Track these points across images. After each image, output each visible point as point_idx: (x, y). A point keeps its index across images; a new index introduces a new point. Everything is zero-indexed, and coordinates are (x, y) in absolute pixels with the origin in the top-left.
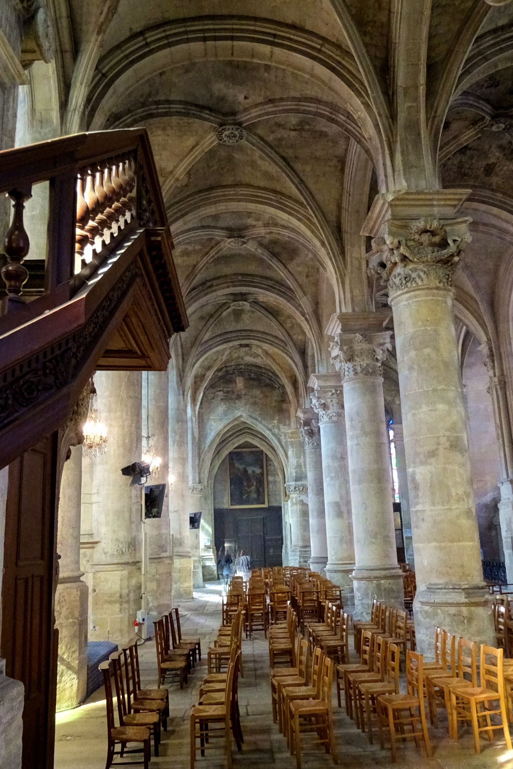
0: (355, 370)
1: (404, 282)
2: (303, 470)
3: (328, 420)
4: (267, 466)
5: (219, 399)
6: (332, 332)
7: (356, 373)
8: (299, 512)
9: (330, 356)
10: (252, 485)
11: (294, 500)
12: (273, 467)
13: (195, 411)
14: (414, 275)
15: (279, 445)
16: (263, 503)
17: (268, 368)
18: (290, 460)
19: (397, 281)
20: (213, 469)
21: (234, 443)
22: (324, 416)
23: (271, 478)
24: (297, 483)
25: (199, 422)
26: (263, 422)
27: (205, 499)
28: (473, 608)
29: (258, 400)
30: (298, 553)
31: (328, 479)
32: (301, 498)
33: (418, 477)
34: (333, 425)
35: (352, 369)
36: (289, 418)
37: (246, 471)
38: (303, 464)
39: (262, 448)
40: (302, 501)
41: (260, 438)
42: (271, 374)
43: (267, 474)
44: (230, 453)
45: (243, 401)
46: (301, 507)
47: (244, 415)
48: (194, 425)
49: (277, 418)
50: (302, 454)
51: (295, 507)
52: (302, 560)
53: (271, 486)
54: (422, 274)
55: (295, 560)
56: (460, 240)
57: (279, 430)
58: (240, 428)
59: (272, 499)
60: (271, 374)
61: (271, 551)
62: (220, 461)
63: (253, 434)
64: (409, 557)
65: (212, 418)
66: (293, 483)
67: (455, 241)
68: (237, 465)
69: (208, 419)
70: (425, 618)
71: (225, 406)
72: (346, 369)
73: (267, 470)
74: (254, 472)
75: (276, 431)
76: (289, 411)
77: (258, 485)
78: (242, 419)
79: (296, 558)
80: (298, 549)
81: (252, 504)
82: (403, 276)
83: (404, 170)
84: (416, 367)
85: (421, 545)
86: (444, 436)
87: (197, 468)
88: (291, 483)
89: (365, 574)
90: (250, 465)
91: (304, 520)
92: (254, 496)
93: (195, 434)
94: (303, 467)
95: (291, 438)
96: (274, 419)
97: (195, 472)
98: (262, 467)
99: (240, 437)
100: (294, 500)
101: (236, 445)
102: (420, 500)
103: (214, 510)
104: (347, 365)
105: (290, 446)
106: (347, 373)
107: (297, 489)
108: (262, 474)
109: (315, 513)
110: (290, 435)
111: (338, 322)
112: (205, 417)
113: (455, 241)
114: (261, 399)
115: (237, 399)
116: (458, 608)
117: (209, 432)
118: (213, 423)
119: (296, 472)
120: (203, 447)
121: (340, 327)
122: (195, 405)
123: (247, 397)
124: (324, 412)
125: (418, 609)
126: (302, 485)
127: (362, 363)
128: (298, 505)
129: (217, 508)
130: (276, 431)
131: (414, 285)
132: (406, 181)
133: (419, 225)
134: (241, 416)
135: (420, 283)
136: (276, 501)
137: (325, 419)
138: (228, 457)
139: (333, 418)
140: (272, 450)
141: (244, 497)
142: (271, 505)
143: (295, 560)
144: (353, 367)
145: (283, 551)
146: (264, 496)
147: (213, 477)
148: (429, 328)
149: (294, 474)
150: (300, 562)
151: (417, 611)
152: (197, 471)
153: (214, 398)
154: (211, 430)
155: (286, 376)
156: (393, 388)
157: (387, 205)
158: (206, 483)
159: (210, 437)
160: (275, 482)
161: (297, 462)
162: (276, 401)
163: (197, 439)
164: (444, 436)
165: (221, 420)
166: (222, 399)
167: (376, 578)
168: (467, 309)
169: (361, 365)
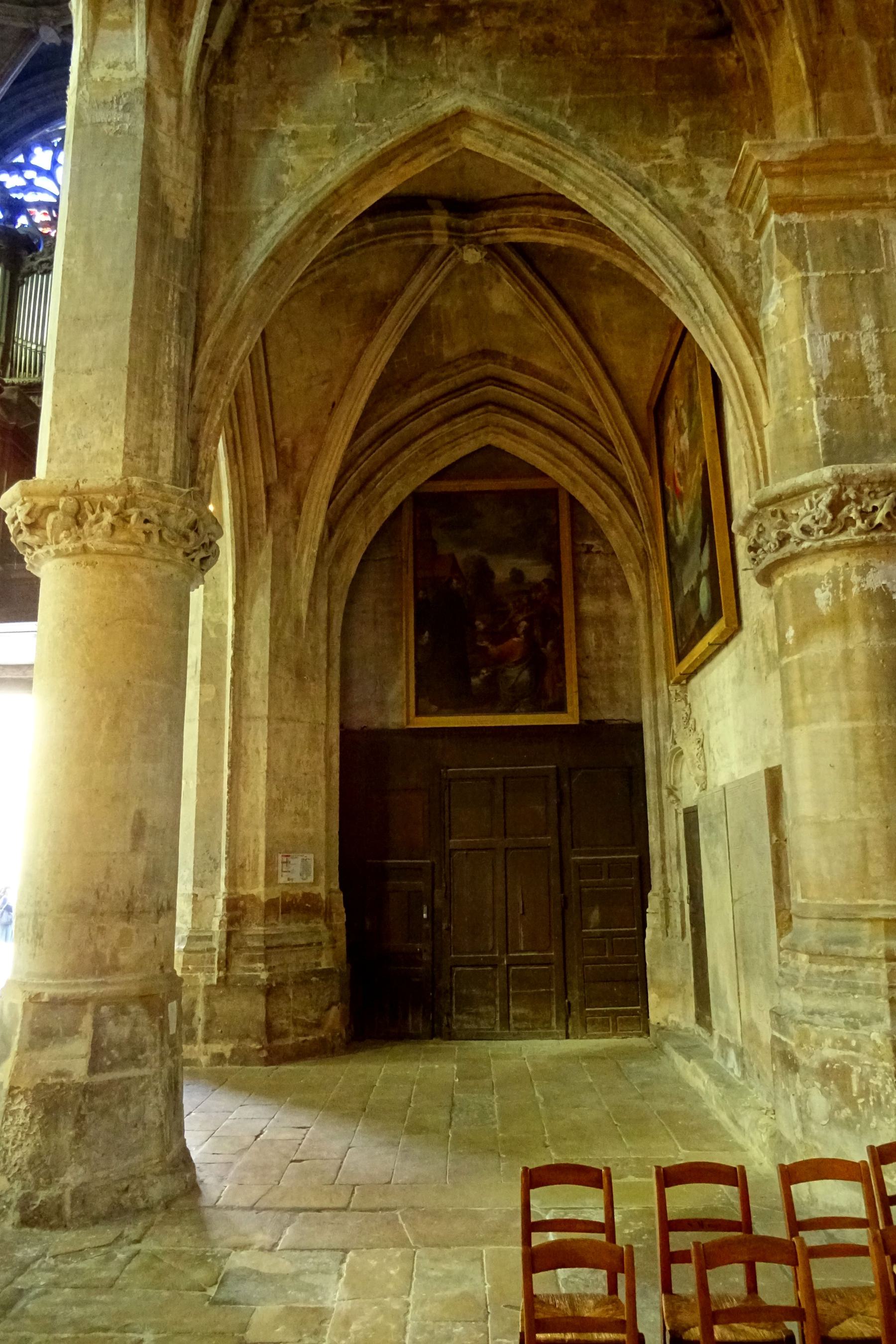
4: (575, 555)
5: (335, 29)
10: (511, 631)
11: (823, 597)
12: (599, 562)
13: (177, 66)
16: (560, 706)
18: (773, 347)
20: (339, 556)
21: (431, 452)
23: (591, 606)
24: (860, 469)
25: (206, 153)
26: (597, 151)
27: (299, 675)
29: (560, 31)
32: (875, 581)
37: (484, 573)
38: (872, 364)
39: (559, 475)
41: (547, 426)
43: (577, 588)
44: (418, 498)
45: (477, 40)
46: (876, 639)
47: (478, 105)
48: (164, 137)
53: (590, 637)
55: (854, 1021)
57: (701, 193)
58: (460, 380)
59: (598, 693)
61: (595, 915)
62: (375, 526)
63: (516, 411)
65: (285, 128)
66: (827, 473)
68: (446, 547)
69: (265, 135)
71: (364, 65)
73: (577, 572)
74: (517, 576)
75: (681, 195)
76: (759, 75)
77: (537, 632)
78: (468, 139)
79: (858, 1004)
81: (510, 709)
87: (168, 389)
88: (805, 478)
90: (502, 547)
92: (519, 675)
93: (166, 187)
94: (876, 382)
95: (780, 204)
97: (155, 414)
98: (552, 557)
99: (461, 423)
100: (823, 597)
101: (442, 462)
103: (348, 737)
105: (778, 258)
108: (554, 585)
110: (781, 186)
112: (242, 122)
114: (583, 27)
115: (437, 27)
117: (265, 203)
118: (293, 158)
119: (829, 416)
120: (222, 289)
122: (180, 32)
123: (497, 19)
128: (859, 632)
129: (356, 726)
130: (681, 195)
134: (462, 117)
136: (614, 698)
138: (407, 514)
140: (598, 477)
141: (475, 681)
142: (593, 716)
143: (854, 1021)
145: (652, 920)
146: (560, 678)
147: (342, 589)
149: (819, 428)
152: (168, 406)
153: (303, 24)
154: (278, 192)
158: (304, 607)
159: (270, 234)
160: (608, 621)
161: (836, 348)
162: (674, 34)
163: (181, 230)
165: (337, 138)
166: (351, 32)
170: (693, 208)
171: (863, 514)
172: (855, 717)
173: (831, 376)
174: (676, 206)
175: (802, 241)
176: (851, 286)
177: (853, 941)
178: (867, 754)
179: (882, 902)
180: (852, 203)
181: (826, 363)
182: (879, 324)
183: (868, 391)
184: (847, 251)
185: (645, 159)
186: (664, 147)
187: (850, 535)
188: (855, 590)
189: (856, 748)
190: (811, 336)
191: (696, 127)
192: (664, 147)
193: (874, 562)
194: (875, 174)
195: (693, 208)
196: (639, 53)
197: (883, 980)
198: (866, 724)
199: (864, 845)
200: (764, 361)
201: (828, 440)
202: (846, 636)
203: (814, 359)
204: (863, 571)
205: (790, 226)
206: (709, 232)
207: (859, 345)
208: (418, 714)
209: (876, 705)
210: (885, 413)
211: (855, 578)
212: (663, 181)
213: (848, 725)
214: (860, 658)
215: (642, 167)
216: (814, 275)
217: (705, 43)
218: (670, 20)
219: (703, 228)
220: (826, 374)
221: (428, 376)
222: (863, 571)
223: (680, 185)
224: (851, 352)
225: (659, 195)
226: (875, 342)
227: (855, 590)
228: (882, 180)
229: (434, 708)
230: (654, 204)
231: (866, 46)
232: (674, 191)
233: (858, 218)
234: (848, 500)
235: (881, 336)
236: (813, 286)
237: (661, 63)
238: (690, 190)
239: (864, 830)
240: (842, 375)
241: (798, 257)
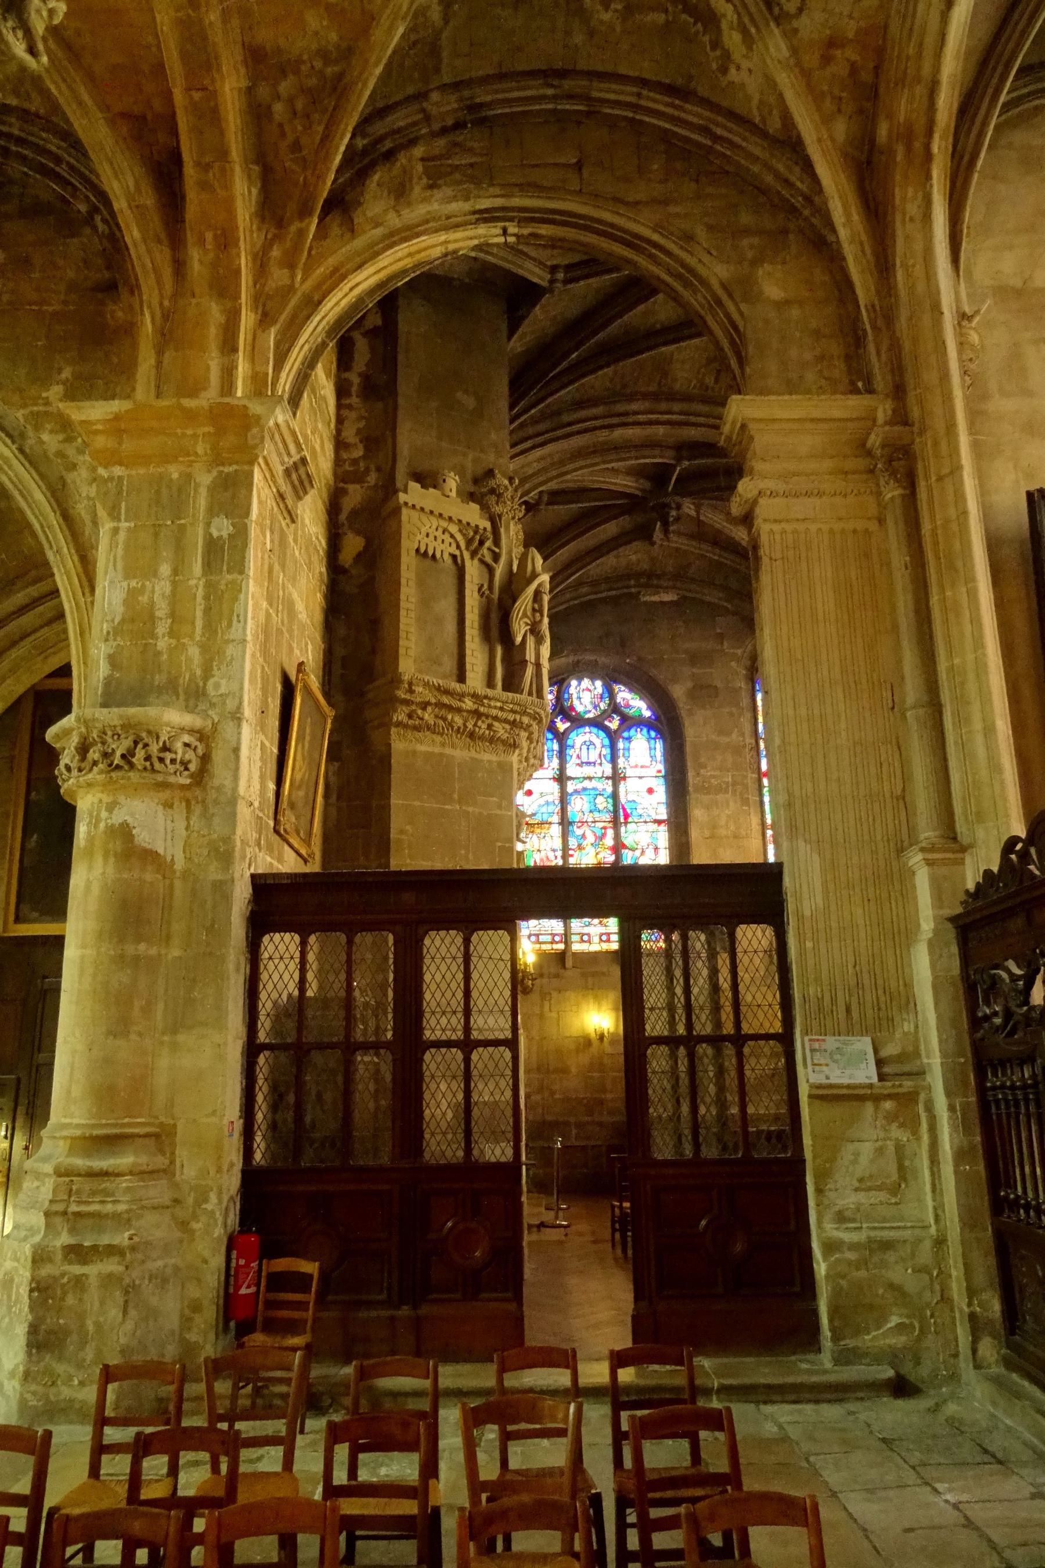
2: (162, 644)
15: (53, 519)
17: (35, 105)
32: (118, 817)
36: (127, 370)
38: (162, 610)
40: (125, 832)
42: (54, 144)
46: (110, 870)
49: (67, 373)
50: (167, 553)
52: (65, 1239)
60: (54, 144)
64: (831, 1230)
91: (120, 960)
94: (162, 629)
96: (45, 382)
107: (94, 754)
126: (128, 726)
150: (40, 1258)
155: (106, 108)
156: (746, 218)
161: (132, 595)
162: (72, 287)
170: (60, 454)
171: (105, 755)
173: (123, 621)
174: (45, 452)
175: (119, 493)
176: (156, 535)
179: (76, 1121)
180: (166, 459)
181: (121, 609)
182: (175, 572)
183: (154, 636)
184: (158, 502)
185: (24, 406)
186: (44, 395)
187: (95, 775)
188: (102, 825)
190: (112, 582)
191: (78, 376)
192: (44, 395)
193: (122, 799)
194: (189, 432)
195: (60, 454)
196: (35, 303)
199: (72, 1069)
200: (92, 603)
201: (108, 682)
202: (90, 868)
203: (110, 604)
204: (111, 808)
205: (111, 479)
206: (70, 477)
207: (153, 592)
208: (18, 920)
209: (100, 935)
210: (165, 657)
211: (104, 814)
212: (37, 428)
214: (96, 889)
215: (20, 414)
216: (124, 525)
217: (100, 295)
218: (71, 274)
219: (64, 473)
220: (117, 621)
221: (33, 573)
223: (51, 432)
224: (144, 599)
225: (31, 441)
226: (168, 590)
227: (102, 825)
228: (195, 436)
229: (35, 915)
230: (21, 450)
231: (213, 305)
232: (45, 437)
233: (174, 472)
234: (94, 743)
235: (174, 584)
236: (122, 536)
237: (54, 314)
238: (61, 437)
240: (133, 620)
241: (114, 508)
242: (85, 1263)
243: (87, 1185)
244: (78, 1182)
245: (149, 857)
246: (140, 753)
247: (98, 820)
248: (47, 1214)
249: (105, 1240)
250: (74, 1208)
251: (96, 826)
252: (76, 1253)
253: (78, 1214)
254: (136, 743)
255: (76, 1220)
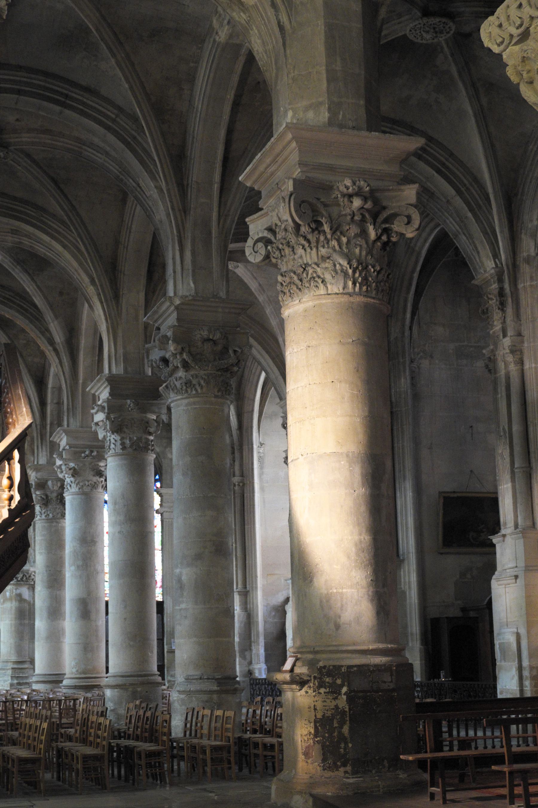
0: (123, 444)
1: (184, 387)
3: (77, 490)
6: (96, 391)
7: (124, 448)
8: (13, 611)
9: (93, 421)
14: (194, 382)
19: (178, 384)
22: (73, 485)
28: (223, 695)
30: (10, 672)
31: (73, 568)
32: (18, 591)
33: (184, 578)
34: (83, 497)
35: (119, 442)
51: (8, 605)
52: (15, 682)
54: (202, 382)
56: (240, 351)
64: (170, 678)
67: (235, 351)
70: (181, 706)
72: (113, 441)
79: (6, 678)
80: (10, 665)
82: (184, 380)
83: (193, 271)
84: (190, 473)
85: (182, 641)
86: (210, 541)
89: (119, 681)
91: (21, 624)
102: (184, 599)
104: (113, 436)
106: (112, 446)
109: (45, 614)
111: (106, 383)
113: (235, 351)
116: (209, 696)
121: (108, 390)
124: (72, 479)
125: (176, 698)
127: (131, 436)
128: (14, 602)
131: (194, 392)
132: (194, 283)
133: (202, 333)
135: (199, 390)
137: (74, 489)
139: (84, 488)
144: (121, 440)
148: (205, 436)
151: (174, 701)
157: (172, 308)
164: (210, 541)
167: (131, 684)
168: (267, 352)
169: (130, 438)
172: (11, 620)
177: (7, 666)
178: (13, 629)
188: (14, 594)
189: (11, 628)
197: (11, 673)
198: (13, 622)
202: (11, 603)
204: (16, 589)
209: (16, 618)
211: (14, 591)
213: (10, 622)
214: (14, 608)
222: (16, 589)
239: (11, 644)
242: (21, 685)
243: (19, 671)
244: (17, 671)
245: (25, 600)
246: (25, 578)
247: (13, 592)
248: (12, 677)
249: (25, 681)
250: (17, 675)
251: (12, 593)
252: (19, 684)
253: (18, 677)
254: (23, 576)
255: (17, 678)
